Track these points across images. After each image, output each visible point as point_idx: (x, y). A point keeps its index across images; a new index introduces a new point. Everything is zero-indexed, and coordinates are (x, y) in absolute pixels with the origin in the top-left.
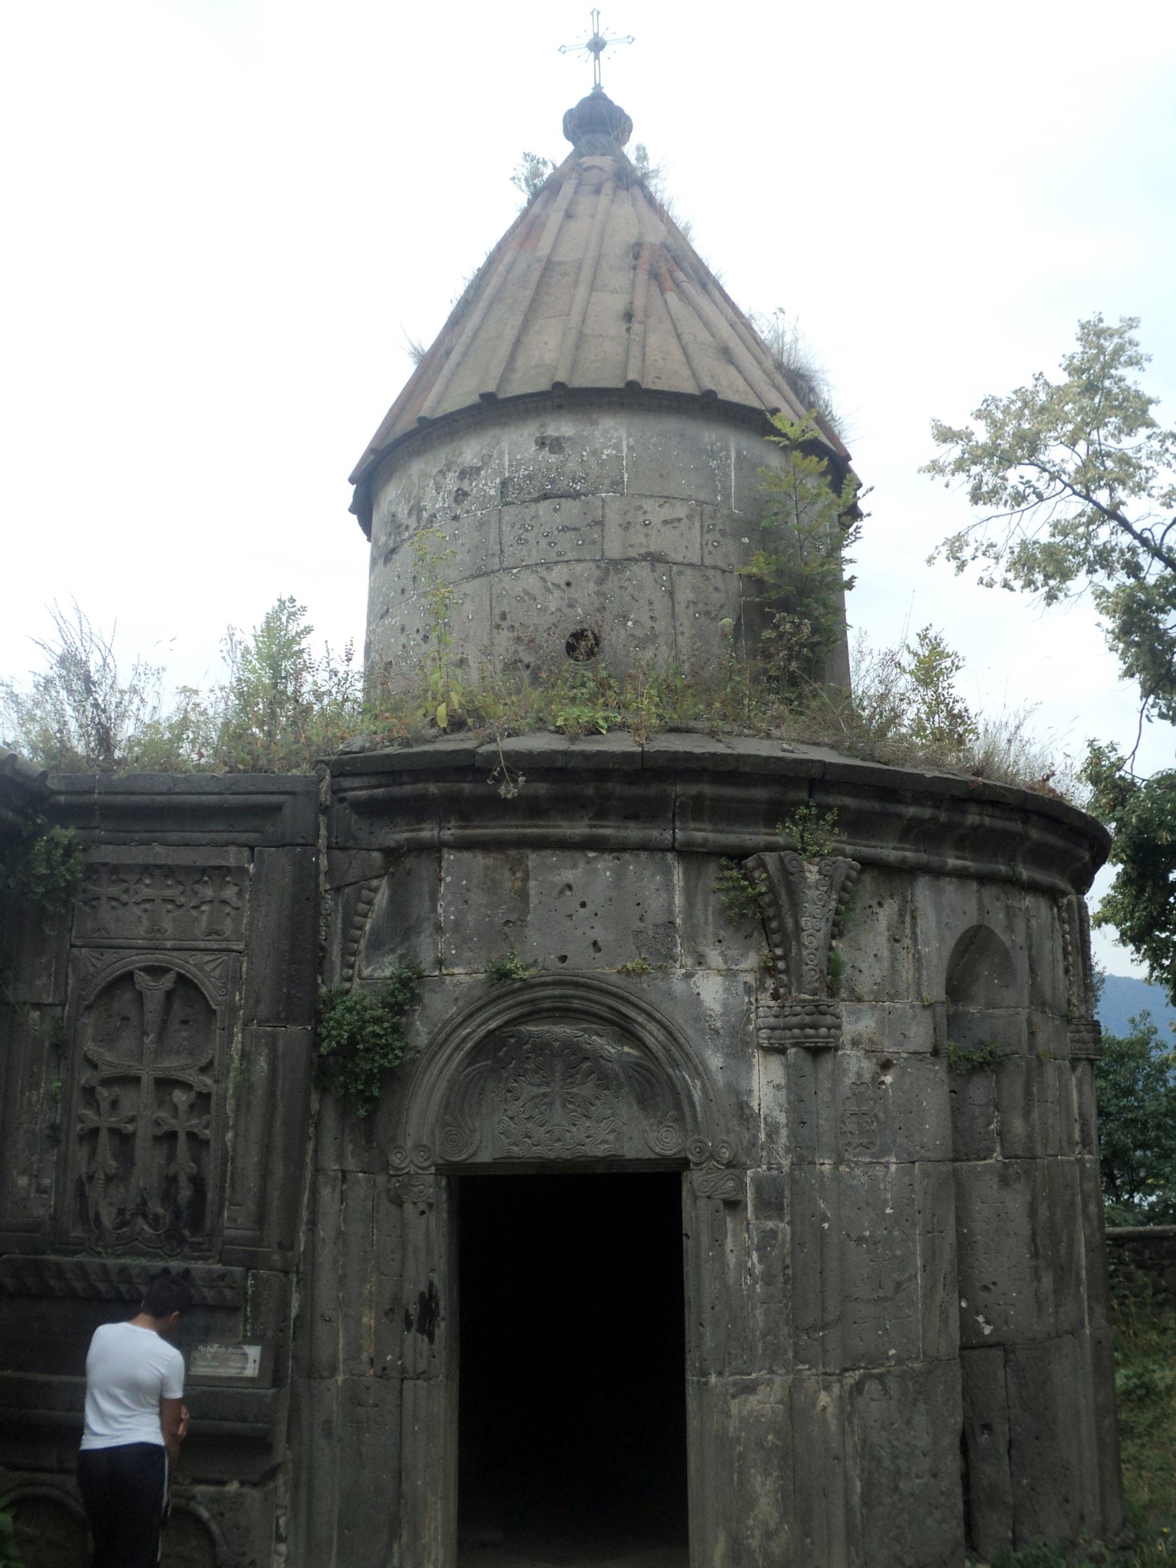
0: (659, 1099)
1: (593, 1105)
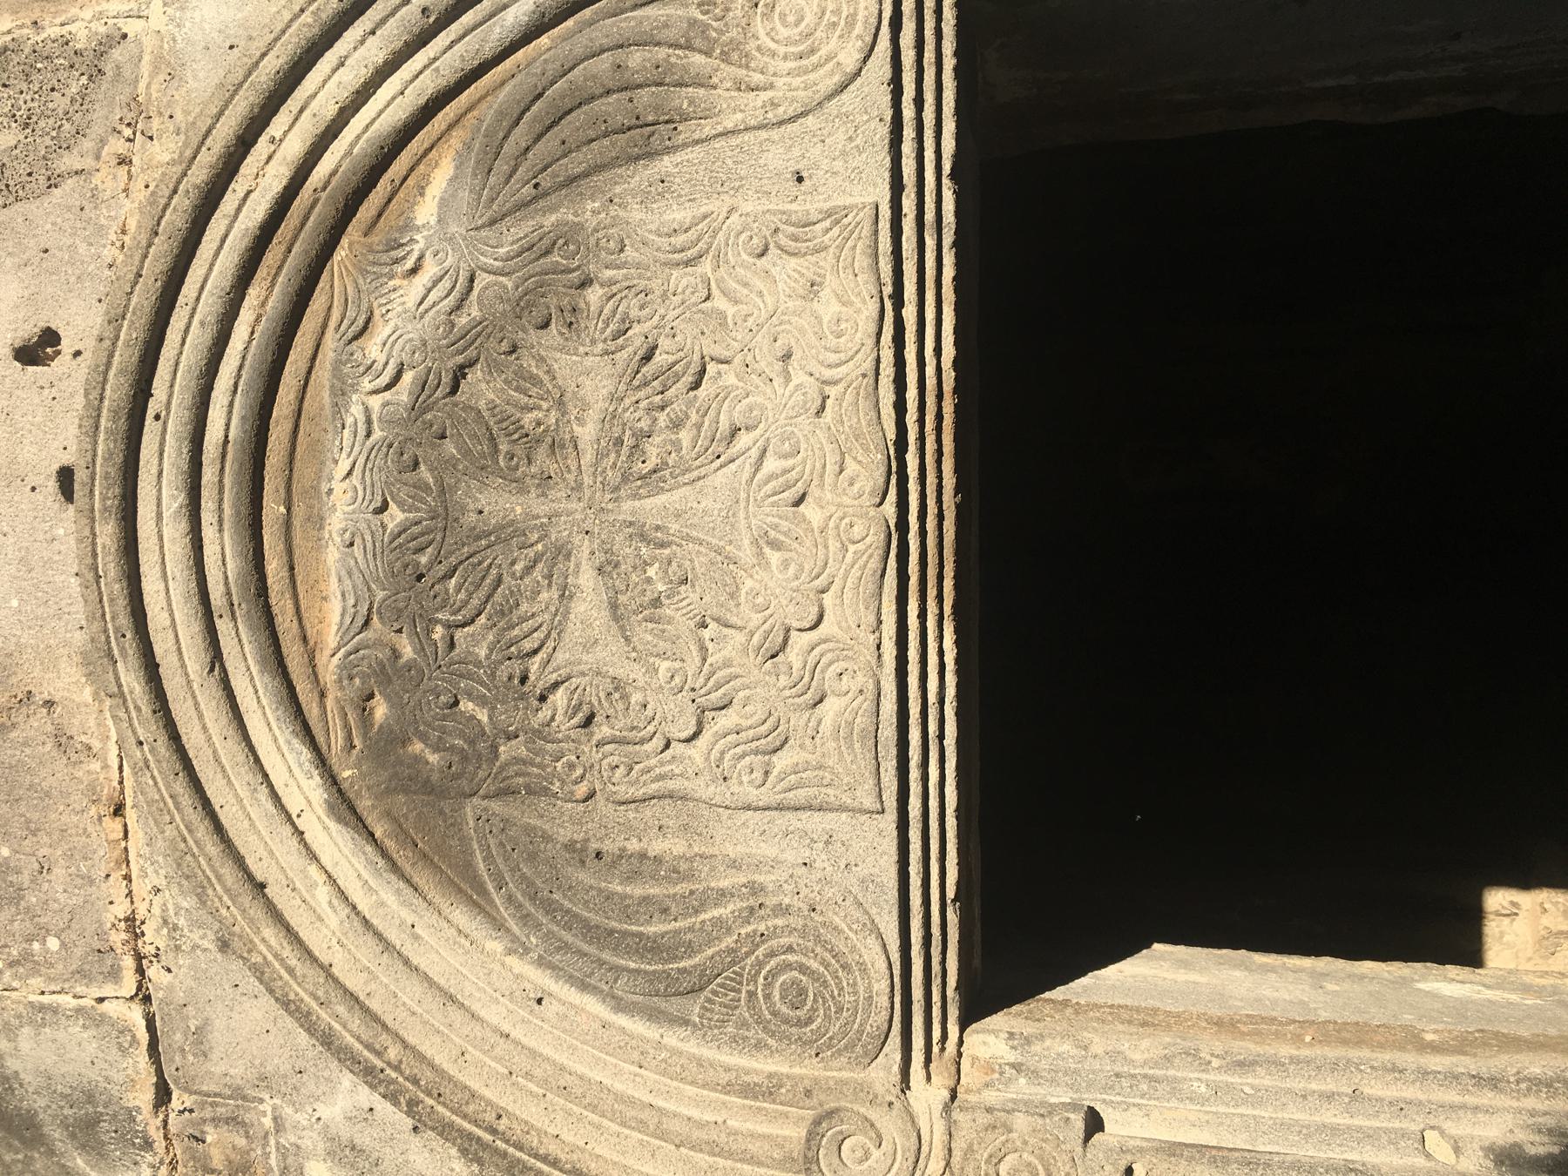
1: (647, 358)
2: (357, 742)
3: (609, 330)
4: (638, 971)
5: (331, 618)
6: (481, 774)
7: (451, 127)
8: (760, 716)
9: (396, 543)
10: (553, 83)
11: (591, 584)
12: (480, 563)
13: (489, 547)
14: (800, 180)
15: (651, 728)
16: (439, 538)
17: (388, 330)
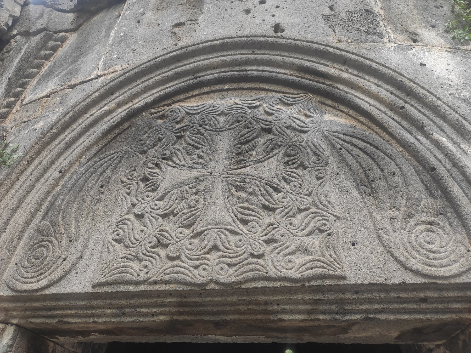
0: (398, 179)
1: (277, 190)
2: (153, 116)
3: (286, 176)
4: (63, 202)
5: (192, 104)
6: (137, 150)
7: (361, 122)
8: (138, 237)
9: (213, 118)
10: (384, 152)
11: (193, 176)
12: (204, 142)
13: (209, 144)
14: (353, 244)
15: (140, 199)
16: (214, 129)
17: (284, 109)
